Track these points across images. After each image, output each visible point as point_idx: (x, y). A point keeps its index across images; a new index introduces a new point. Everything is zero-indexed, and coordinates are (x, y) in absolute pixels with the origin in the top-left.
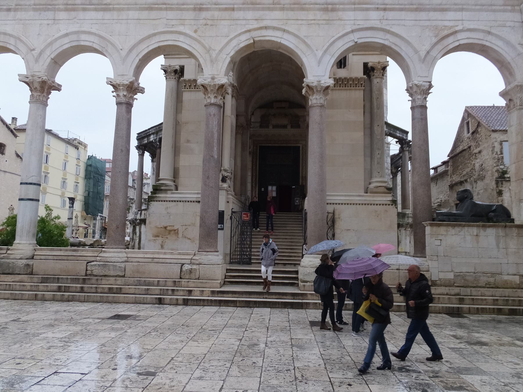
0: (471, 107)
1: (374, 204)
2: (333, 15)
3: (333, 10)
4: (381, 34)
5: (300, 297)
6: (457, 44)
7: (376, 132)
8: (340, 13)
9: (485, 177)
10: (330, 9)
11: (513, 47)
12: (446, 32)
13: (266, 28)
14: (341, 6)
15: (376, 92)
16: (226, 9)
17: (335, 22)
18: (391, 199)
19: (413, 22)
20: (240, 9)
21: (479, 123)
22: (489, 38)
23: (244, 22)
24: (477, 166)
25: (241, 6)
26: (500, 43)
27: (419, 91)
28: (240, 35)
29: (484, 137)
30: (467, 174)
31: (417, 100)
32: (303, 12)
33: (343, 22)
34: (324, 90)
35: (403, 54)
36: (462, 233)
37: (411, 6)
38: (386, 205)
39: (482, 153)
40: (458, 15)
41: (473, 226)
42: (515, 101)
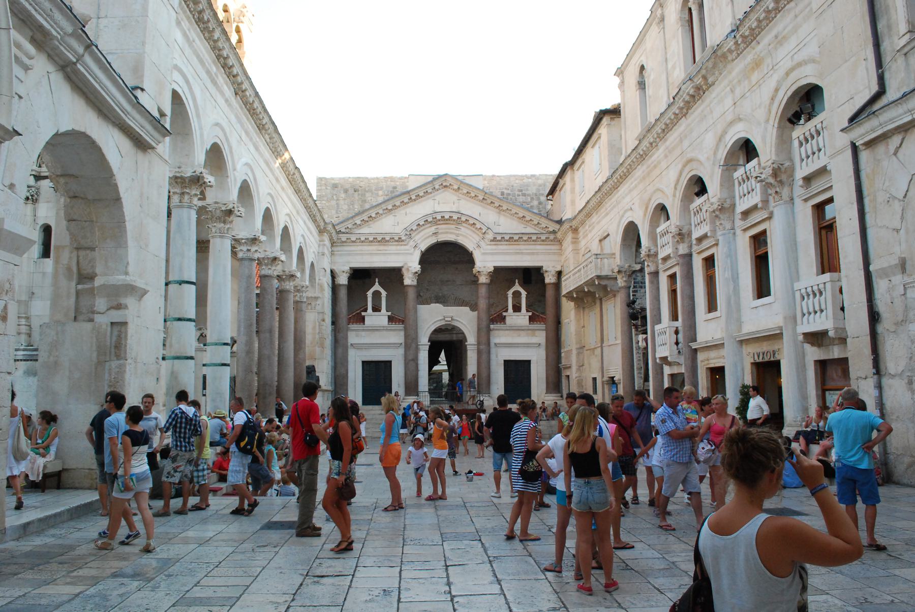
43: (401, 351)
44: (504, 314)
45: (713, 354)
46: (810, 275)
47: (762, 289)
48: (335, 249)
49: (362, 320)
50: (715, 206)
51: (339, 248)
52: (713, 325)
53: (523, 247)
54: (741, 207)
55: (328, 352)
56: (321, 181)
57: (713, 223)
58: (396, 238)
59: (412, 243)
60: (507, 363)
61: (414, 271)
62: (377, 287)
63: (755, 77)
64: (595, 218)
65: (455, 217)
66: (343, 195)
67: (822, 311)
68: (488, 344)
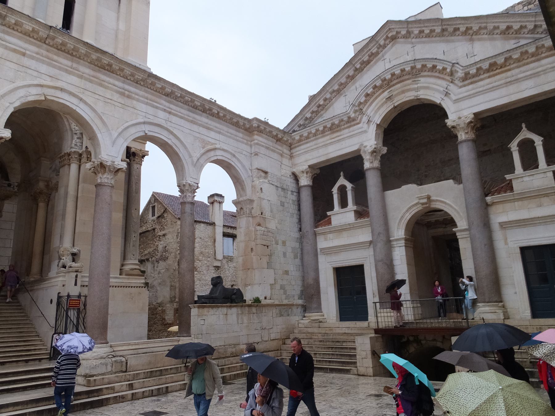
0: (158, 193)
1: (129, 287)
2: (128, 102)
3: (129, 97)
4: (165, 133)
5: (95, 394)
6: (215, 158)
7: (133, 215)
8: (135, 102)
9: (167, 258)
10: (126, 95)
11: (246, 170)
12: (210, 147)
13: (62, 90)
14: (137, 97)
15: (136, 177)
16: (15, 51)
17: (129, 108)
18: (143, 281)
19: (188, 131)
20: (32, 58)
21: (166, 209)
22: (234, 159)
23: (35, 74)
24: (160, 248)
25: (34, 55)
26: (239, 165)
27: (190, 190)
28: (29, 86)
29: (169, 222)
30: (149, 253)
31: (187, 197)
32: (102, 88)
33: (136, 111)
34: (115, 172)
35: (181, 155)
36: (217, 313)
37: (189, 118)
38: (140, 287)
39: (166, 237)
40: (217, 136)
41: (224, 307)
42: (245, 209)
44: (508, 177)
48: (293, 151)
51: (297, 149)
53: (516, 73)
58: (345, 119)
59: (365, 119)
60: (526, 252)
61: (370, 150)
62: (342, 181)
65: (408, 69)
68: (486, 225)
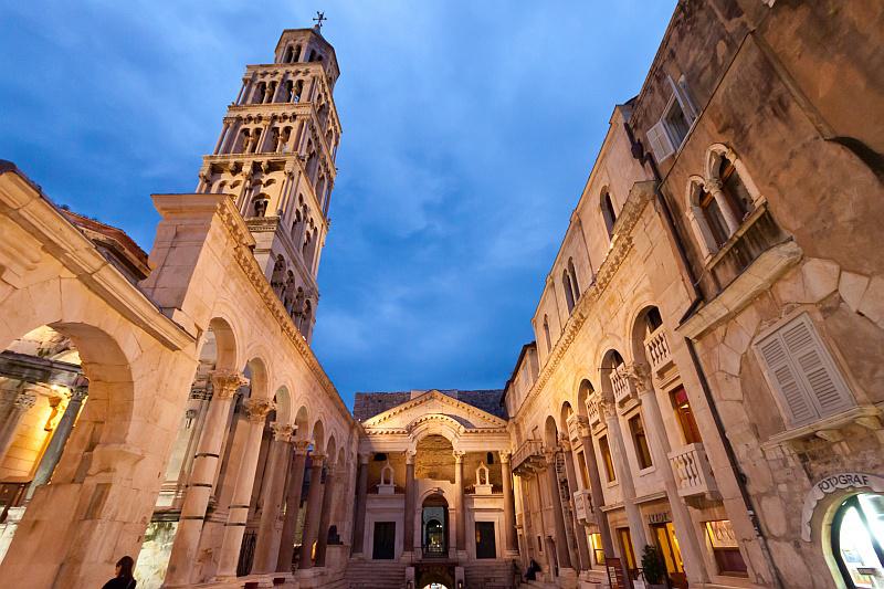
43: (402, 514)
45: (618, 515)
46: (679, 446)
47: (645, 461)
49: (376, 490)
50: (600, 399)
52: (614, 491)
54: (618, 399)
55: (350, 515)
56: (359, 395)
57: (601, 412)
63: (612, 309)
64: (528, 416)
66: (371, 404)
67: (695, 477)
